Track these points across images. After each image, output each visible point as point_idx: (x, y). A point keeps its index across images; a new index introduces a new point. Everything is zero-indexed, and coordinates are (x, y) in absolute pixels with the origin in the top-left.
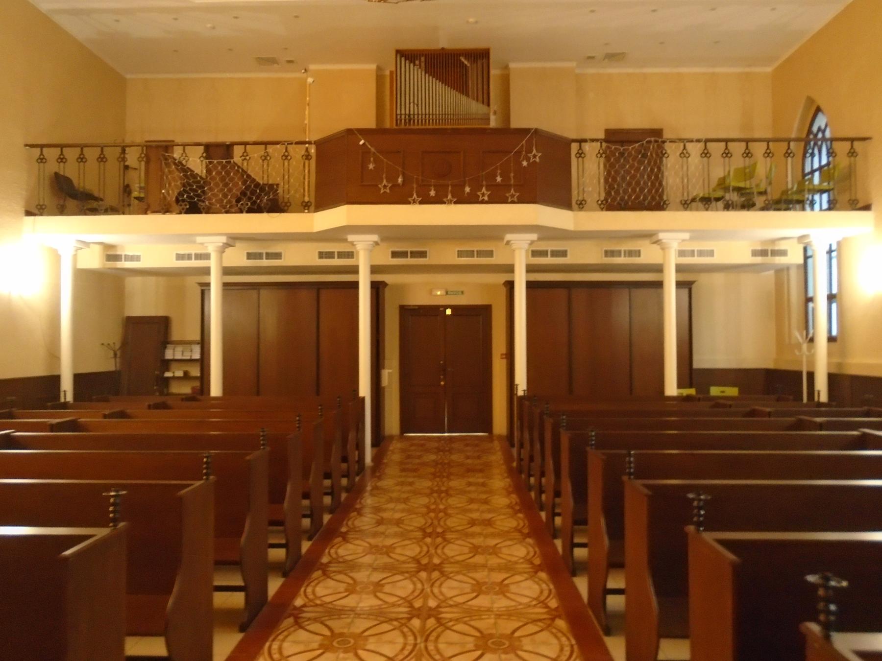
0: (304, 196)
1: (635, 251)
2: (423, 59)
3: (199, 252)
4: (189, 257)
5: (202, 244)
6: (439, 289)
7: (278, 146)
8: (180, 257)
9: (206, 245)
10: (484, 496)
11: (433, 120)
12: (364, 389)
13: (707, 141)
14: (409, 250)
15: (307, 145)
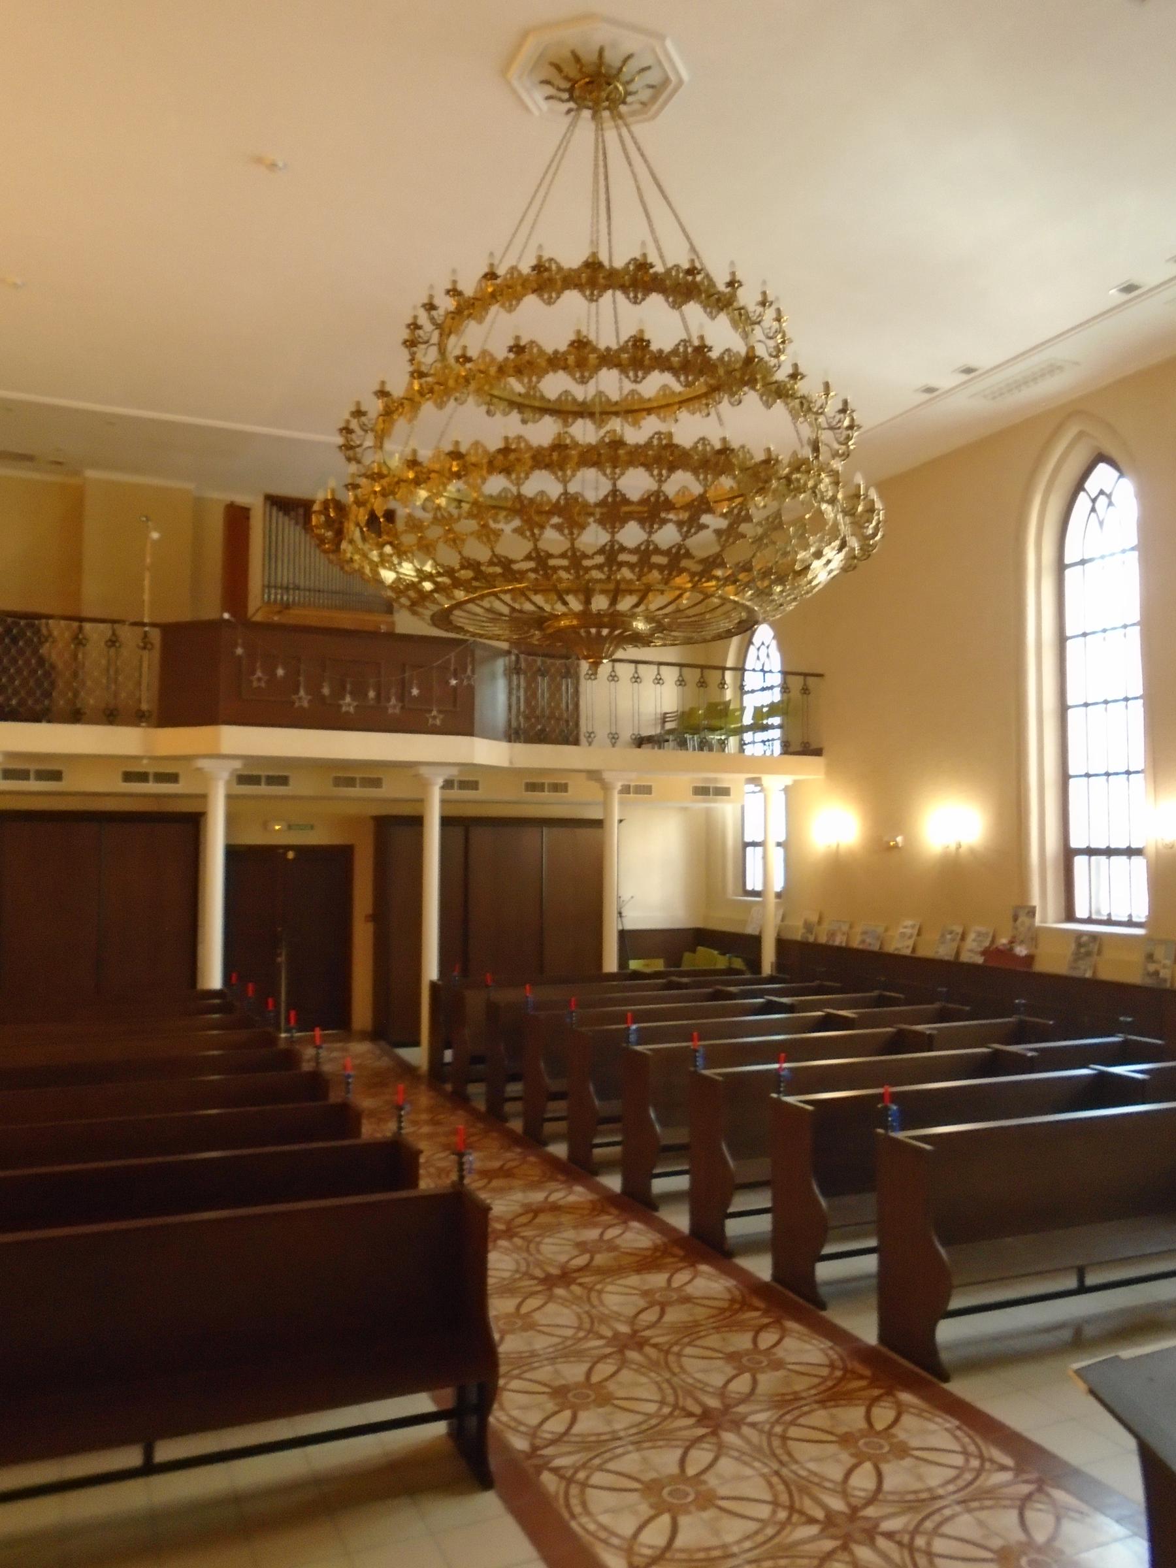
6: (278, 821)
7: (102, 626)
13: (660, 664)
15: (147, 629)
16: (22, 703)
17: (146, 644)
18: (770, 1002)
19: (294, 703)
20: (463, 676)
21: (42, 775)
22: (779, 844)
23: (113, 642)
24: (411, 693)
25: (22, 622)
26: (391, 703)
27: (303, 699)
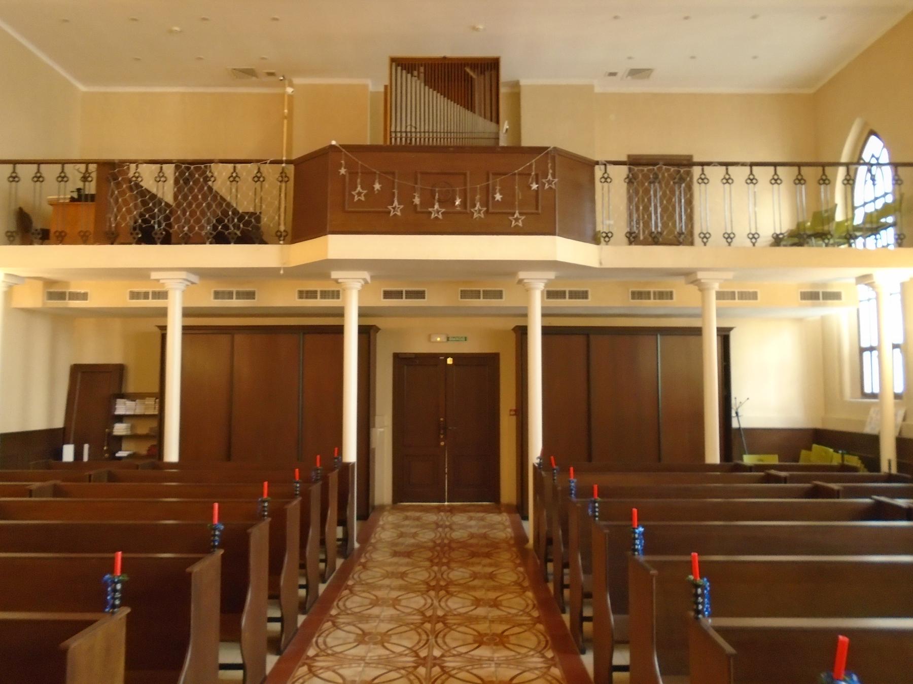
0: (279, 224)
1: (667, 293)
2: (422, 69)
3: (157, 289)
4: (146, 296)
5: (158, 280)
6: (438, 334)
7: (249, 165)
8: (134, 295)
9: (161, 281)
10: (492, 595)
11: (433, 139)
12: (351, 454)
13: (752, 165)
14: (404, 289)
15: (284, 165)
16: (191, 229)
17: (283, 176)
18: (879, 503)
19: (389, 212)
20: (544, 181)
21: (242, 295)
22: (895, 346)
23: (258, 178)
24: (494, 198)
25: (192, 167)
26: (476, 208)
27: (396, 208)
